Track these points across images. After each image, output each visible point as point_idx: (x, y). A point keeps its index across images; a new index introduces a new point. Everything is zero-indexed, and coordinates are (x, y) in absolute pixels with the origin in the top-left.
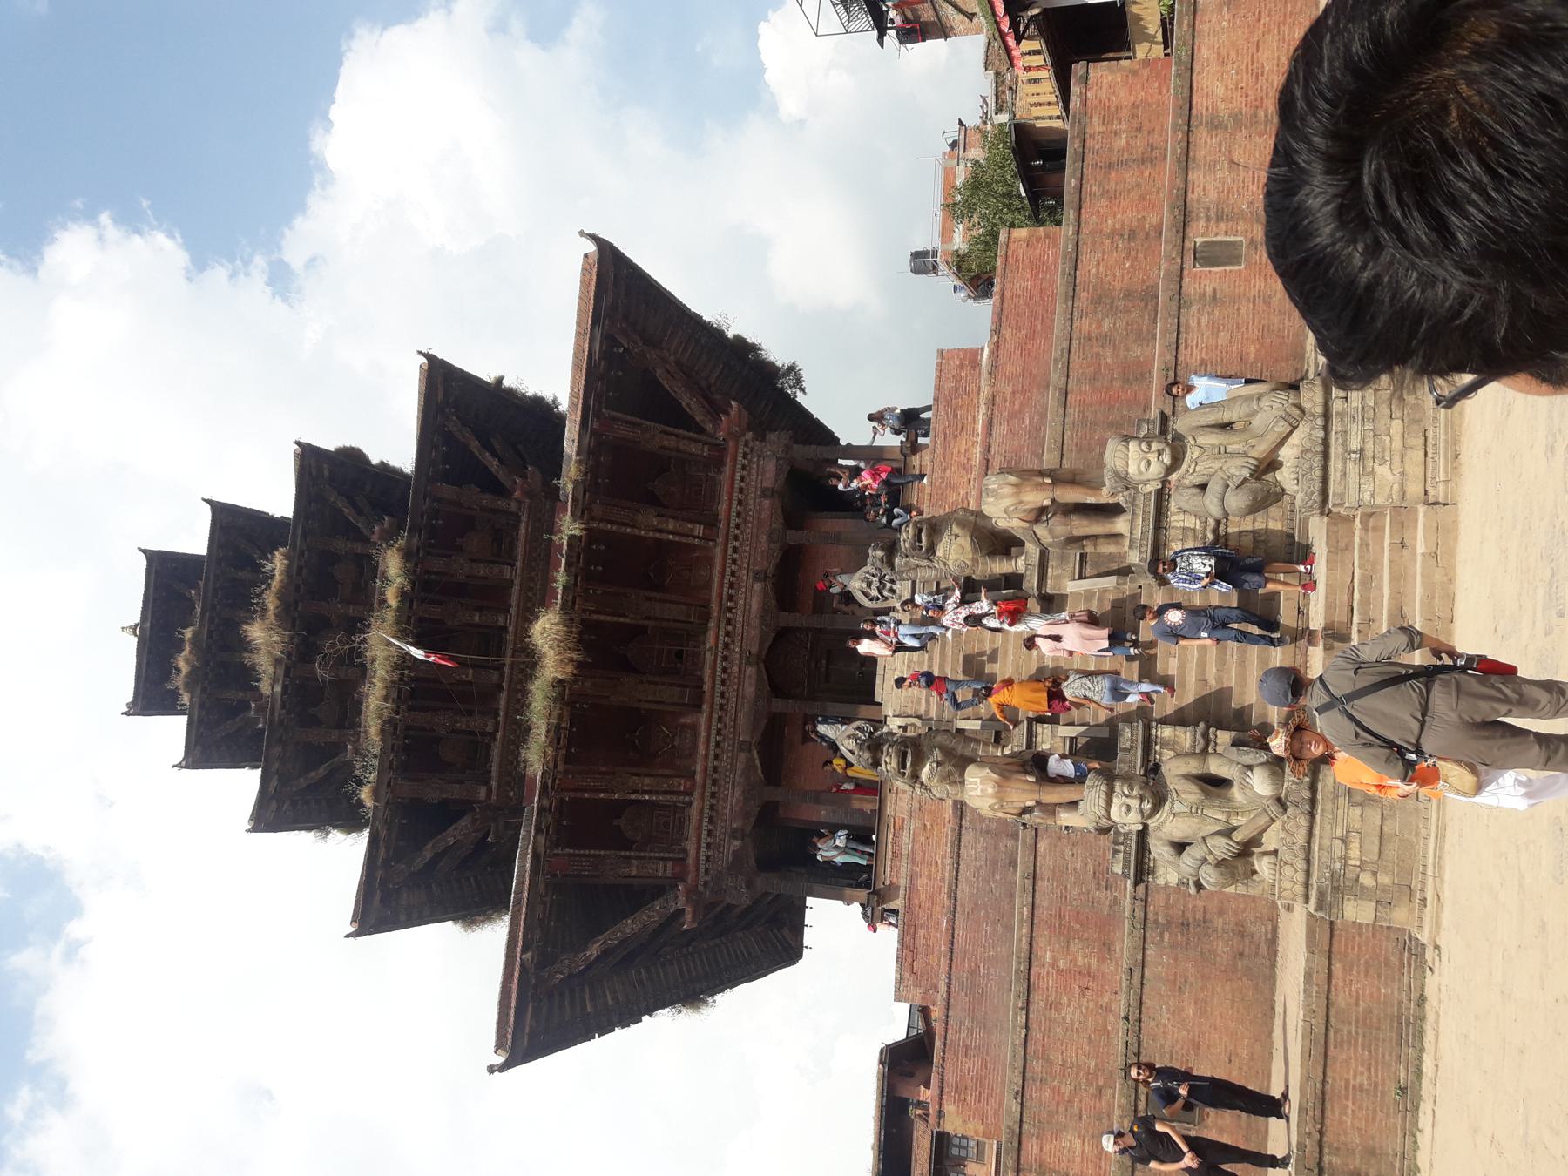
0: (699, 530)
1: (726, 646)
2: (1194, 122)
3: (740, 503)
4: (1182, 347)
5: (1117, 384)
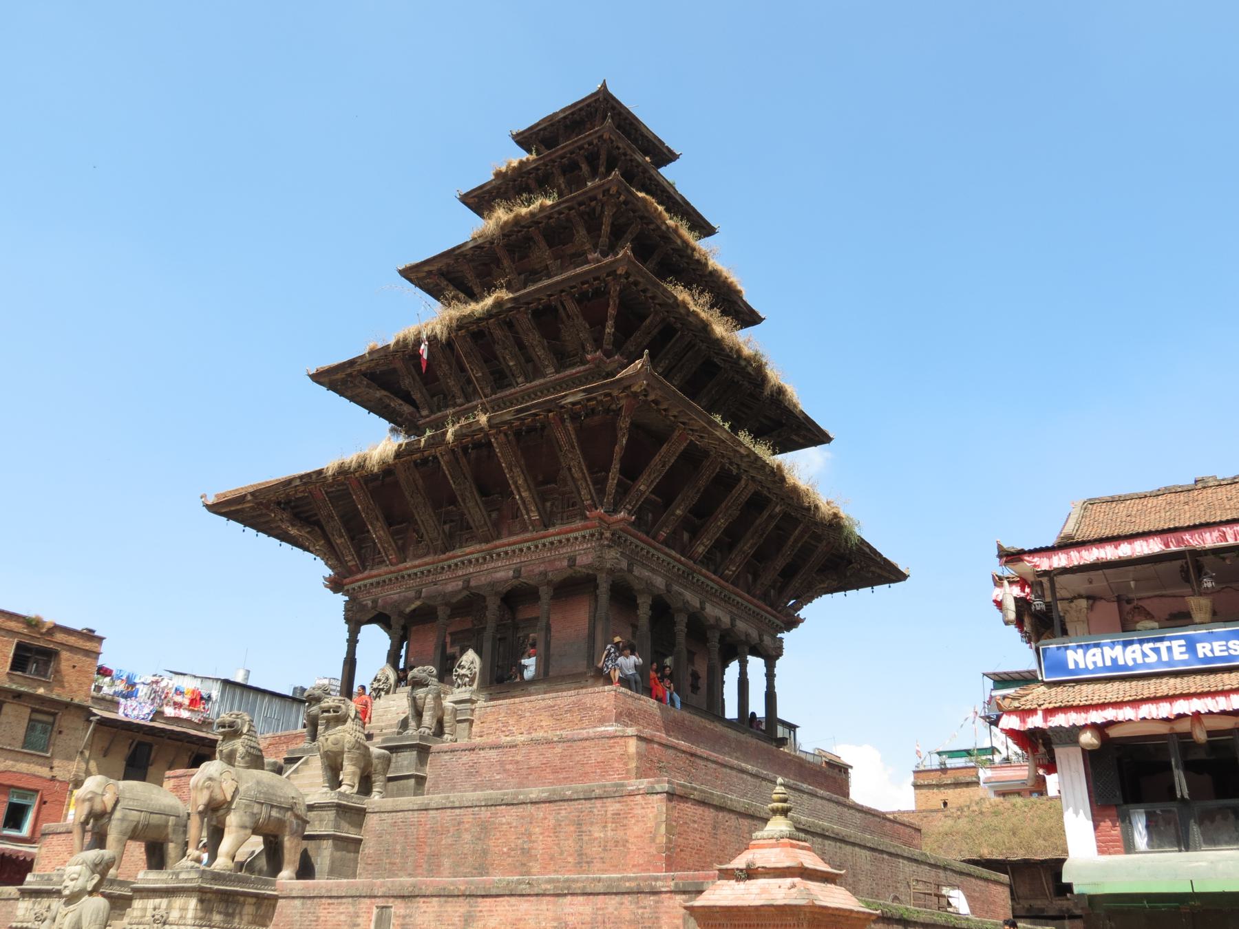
0: (535, 516)
1: (470, 561)
2: (472, 900)
3: (560, 542)
4: (330, 901)
5: (428, 850)
